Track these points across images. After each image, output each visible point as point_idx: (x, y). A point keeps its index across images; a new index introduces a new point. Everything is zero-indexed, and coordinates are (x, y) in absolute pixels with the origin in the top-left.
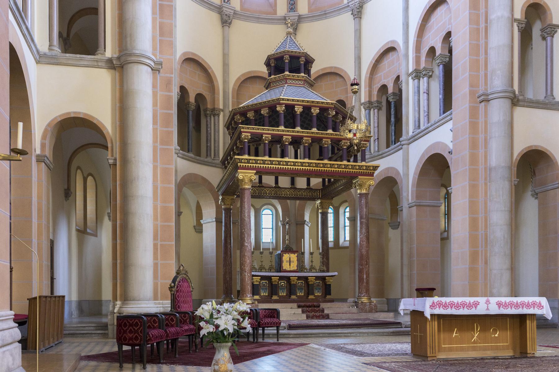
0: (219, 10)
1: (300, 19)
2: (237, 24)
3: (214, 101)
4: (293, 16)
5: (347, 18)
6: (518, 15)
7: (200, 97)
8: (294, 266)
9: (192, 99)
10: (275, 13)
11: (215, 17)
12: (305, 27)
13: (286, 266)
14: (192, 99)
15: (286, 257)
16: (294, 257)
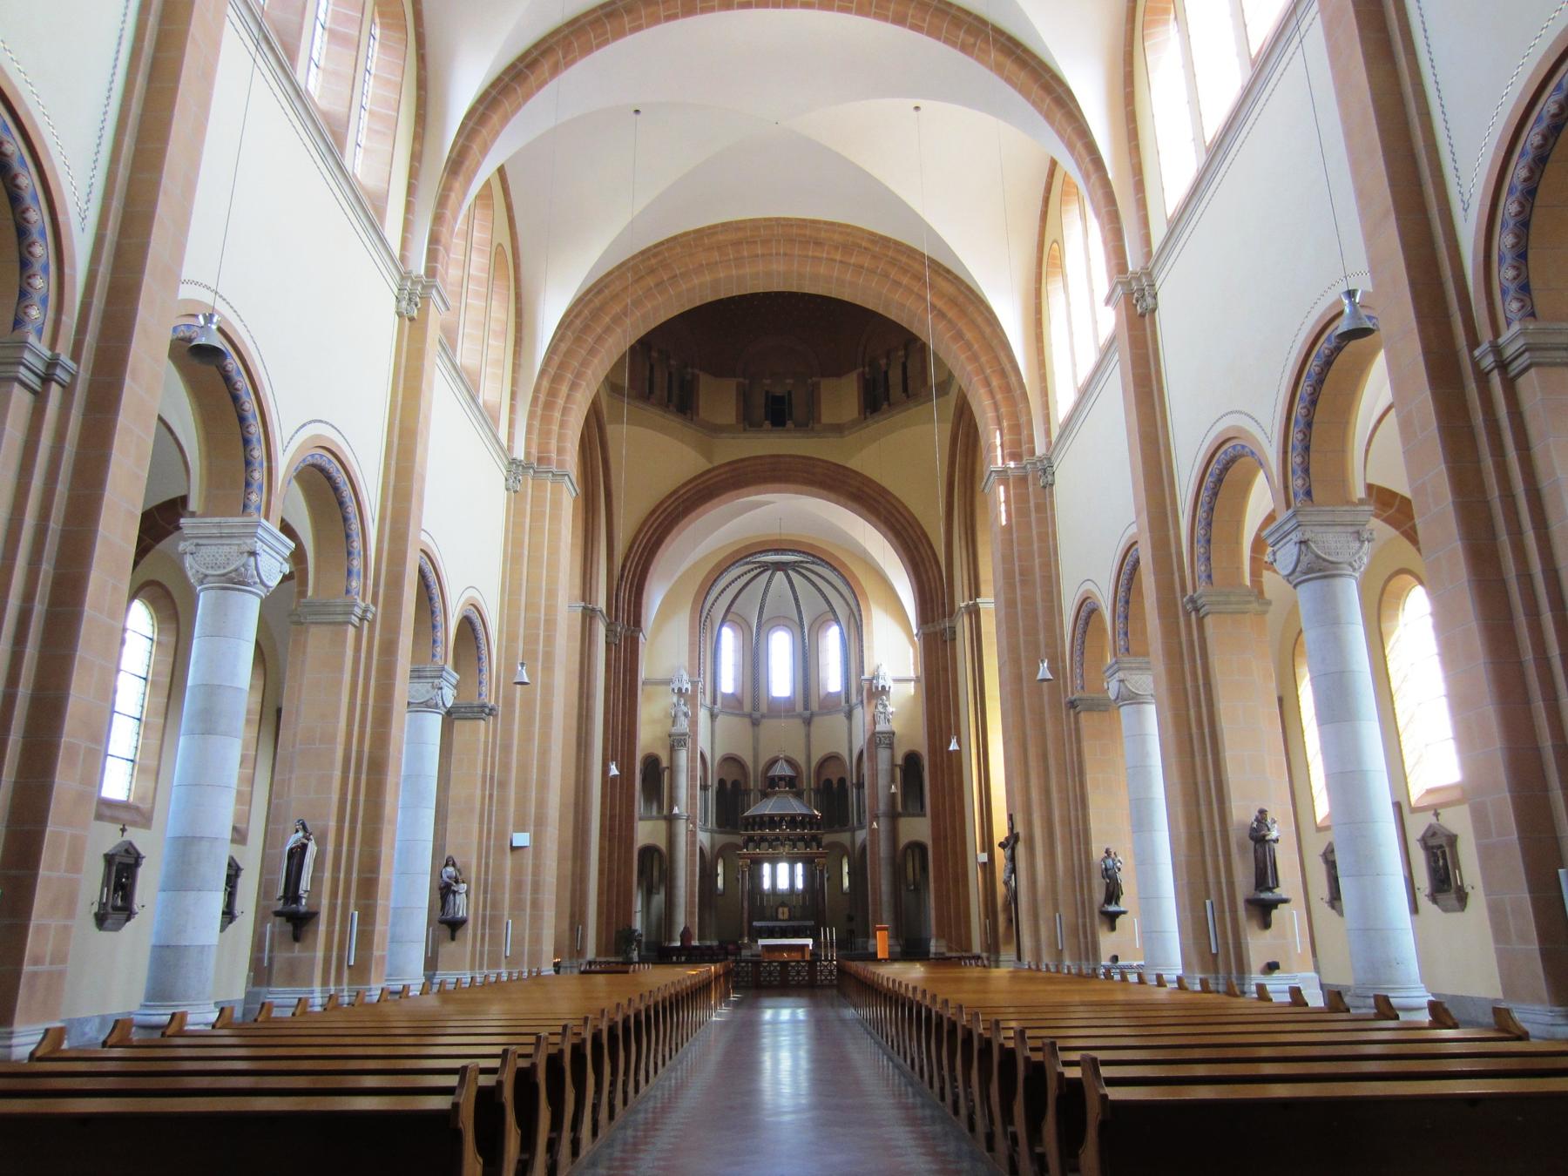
0: (750, 716)
1: (812, 715)
2: (765, 723)
3: (746, 782)
4: (808, 713)
5: (842, 717)
6: (899, 761)
7: (735, 783)
8: (786, 916)
9: (729, 786)
10: (794, 710)
11: (747, 721)
12: (816, 721)
13: (780, 916)
14: (729, 786)
15: (780, 910)
16: (786, 910)
